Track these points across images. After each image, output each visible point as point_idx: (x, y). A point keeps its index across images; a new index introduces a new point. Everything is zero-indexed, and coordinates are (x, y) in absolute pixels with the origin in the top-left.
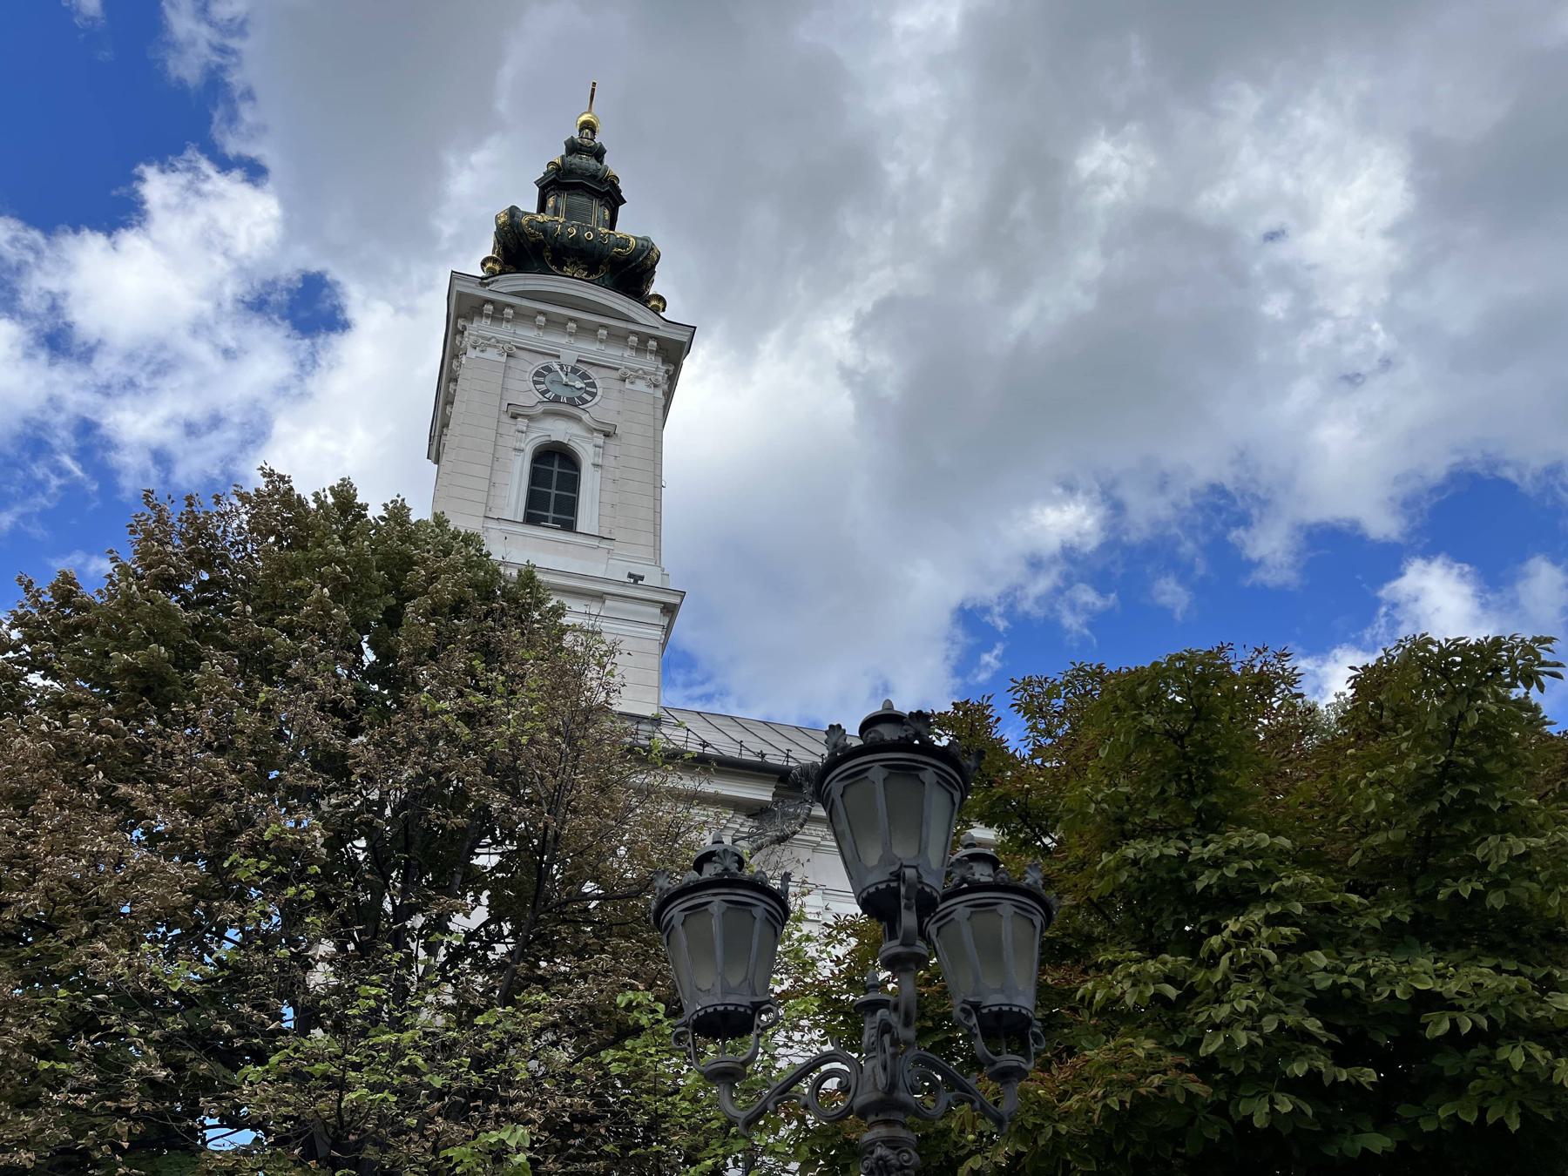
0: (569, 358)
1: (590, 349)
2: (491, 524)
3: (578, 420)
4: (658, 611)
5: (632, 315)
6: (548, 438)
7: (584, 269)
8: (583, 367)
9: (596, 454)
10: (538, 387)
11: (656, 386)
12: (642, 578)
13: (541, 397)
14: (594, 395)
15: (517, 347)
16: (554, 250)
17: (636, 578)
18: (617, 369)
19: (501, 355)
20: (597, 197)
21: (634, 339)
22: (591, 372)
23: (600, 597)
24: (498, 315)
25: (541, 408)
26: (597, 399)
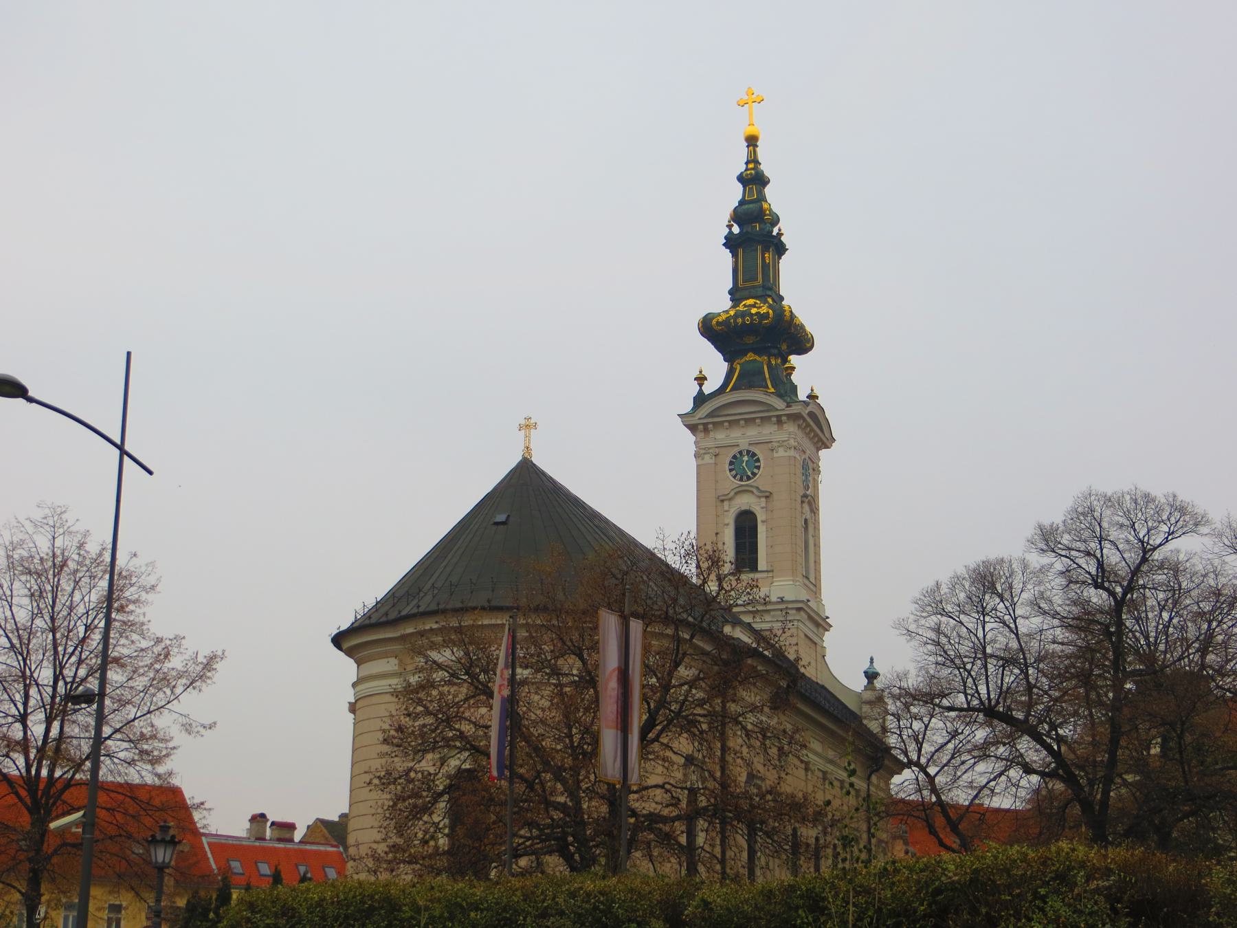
0: (744, 446)
1: (753, 433)
3: (752, 492)
13: (733, 479)
17: (782, 599)
21: (774, 419)
22: (757, 451)
25: (732, 494)
26: (761, 469)
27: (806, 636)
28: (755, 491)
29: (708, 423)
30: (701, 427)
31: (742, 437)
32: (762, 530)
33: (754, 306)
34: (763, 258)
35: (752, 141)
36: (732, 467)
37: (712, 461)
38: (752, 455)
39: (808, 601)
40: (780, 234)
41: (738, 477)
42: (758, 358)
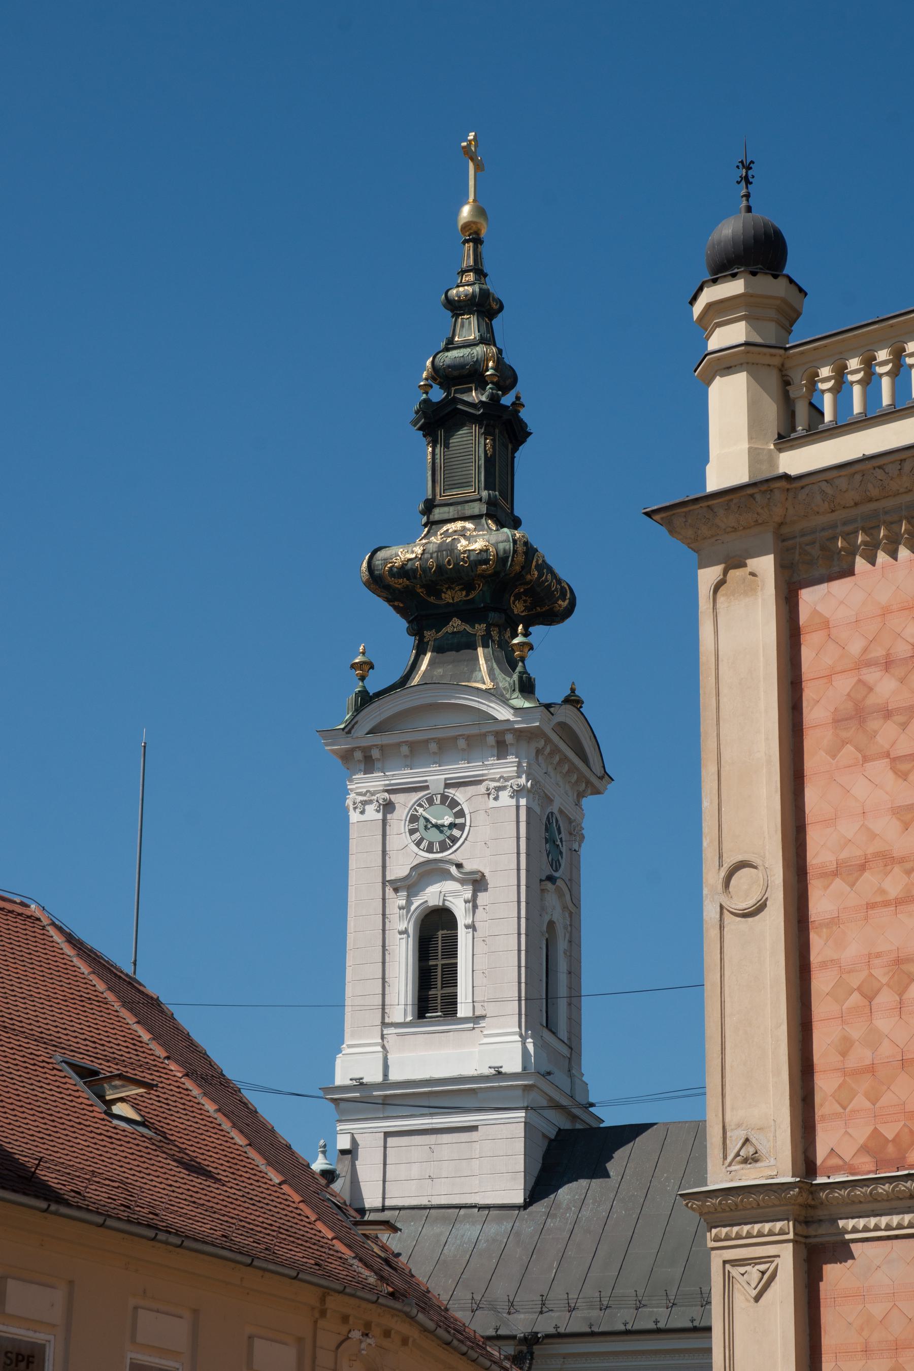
4: (519, 1092)
6: (425, 905)
7: (461, 590)
8: (451, 792)
14: (461, 827)
19: (378, 811)
21: (491, 740)
22: (459, 795)
26: (467, 829)
28: (453, 870)
29: (370, 748)
32: (463, 937)
33: (462, 533)
36: (415, 826)
39: (549, 1073)
40: (518, 404)
41: (425, 844)
42: (468, 629)
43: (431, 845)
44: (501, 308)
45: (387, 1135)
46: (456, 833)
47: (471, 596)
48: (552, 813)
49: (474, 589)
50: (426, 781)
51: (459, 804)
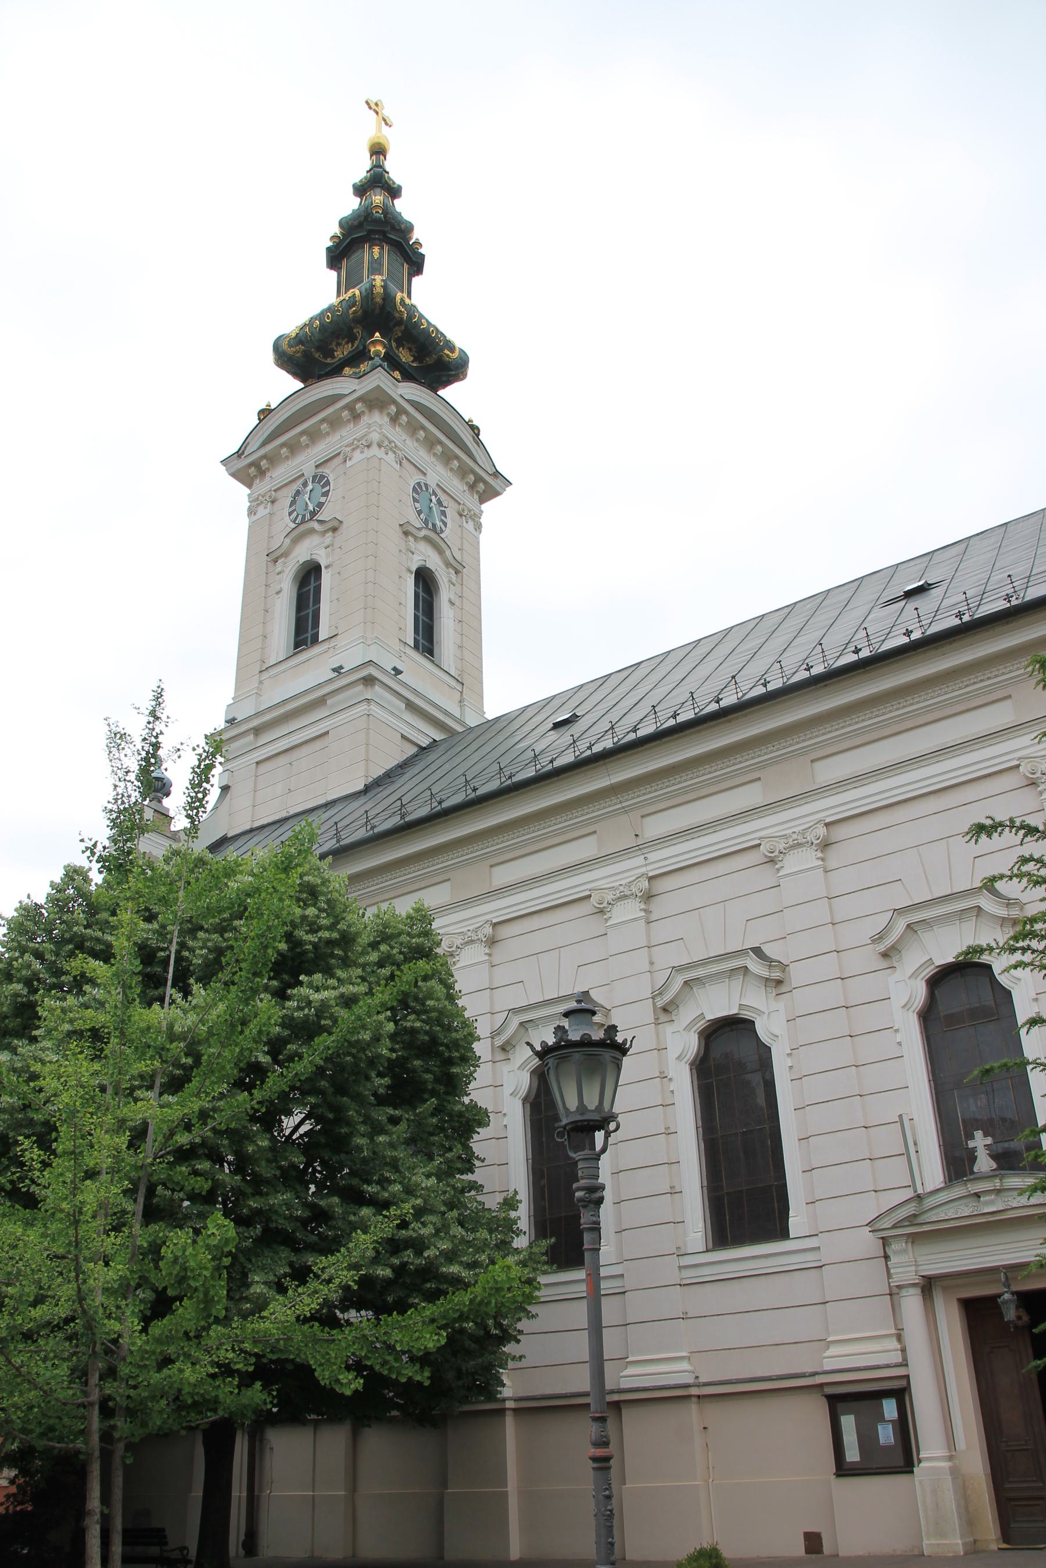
0: (309, 470)
1: (320, 450)
2: (265, 675)
3: (312, 531)
4: (361, 687)
5: (336, 392)
6: (298, 565)
7: (347, 343)
9: (328, 556)
10: (291, 517)
11: (368, 447)
12: (341, 667)
14: (326, 494)
15: (275, 491)
16: (319, 349)
17: (337, 670)
18: (339, 454)
19: (265, 508)
20: (366, 242)
21: (345, 414)
22: (326, 470)
23: (321, 702)
24: (262, 473)
25: (288, 541)
27: (403, 736)
30: (252, 471)
31: (305, 462)
32: (326, 577)
34: (371, 254)
35: (378, 151)
37: (268, 511)
38: (320, 479)
43: (304, 516)
44: (399, 188)
45: (257, 763)
46: (323, 499)
47: (356, 345)
48: (426, 485)
49: (356, 339)
50: (301, 470)
51: (325, 477)
